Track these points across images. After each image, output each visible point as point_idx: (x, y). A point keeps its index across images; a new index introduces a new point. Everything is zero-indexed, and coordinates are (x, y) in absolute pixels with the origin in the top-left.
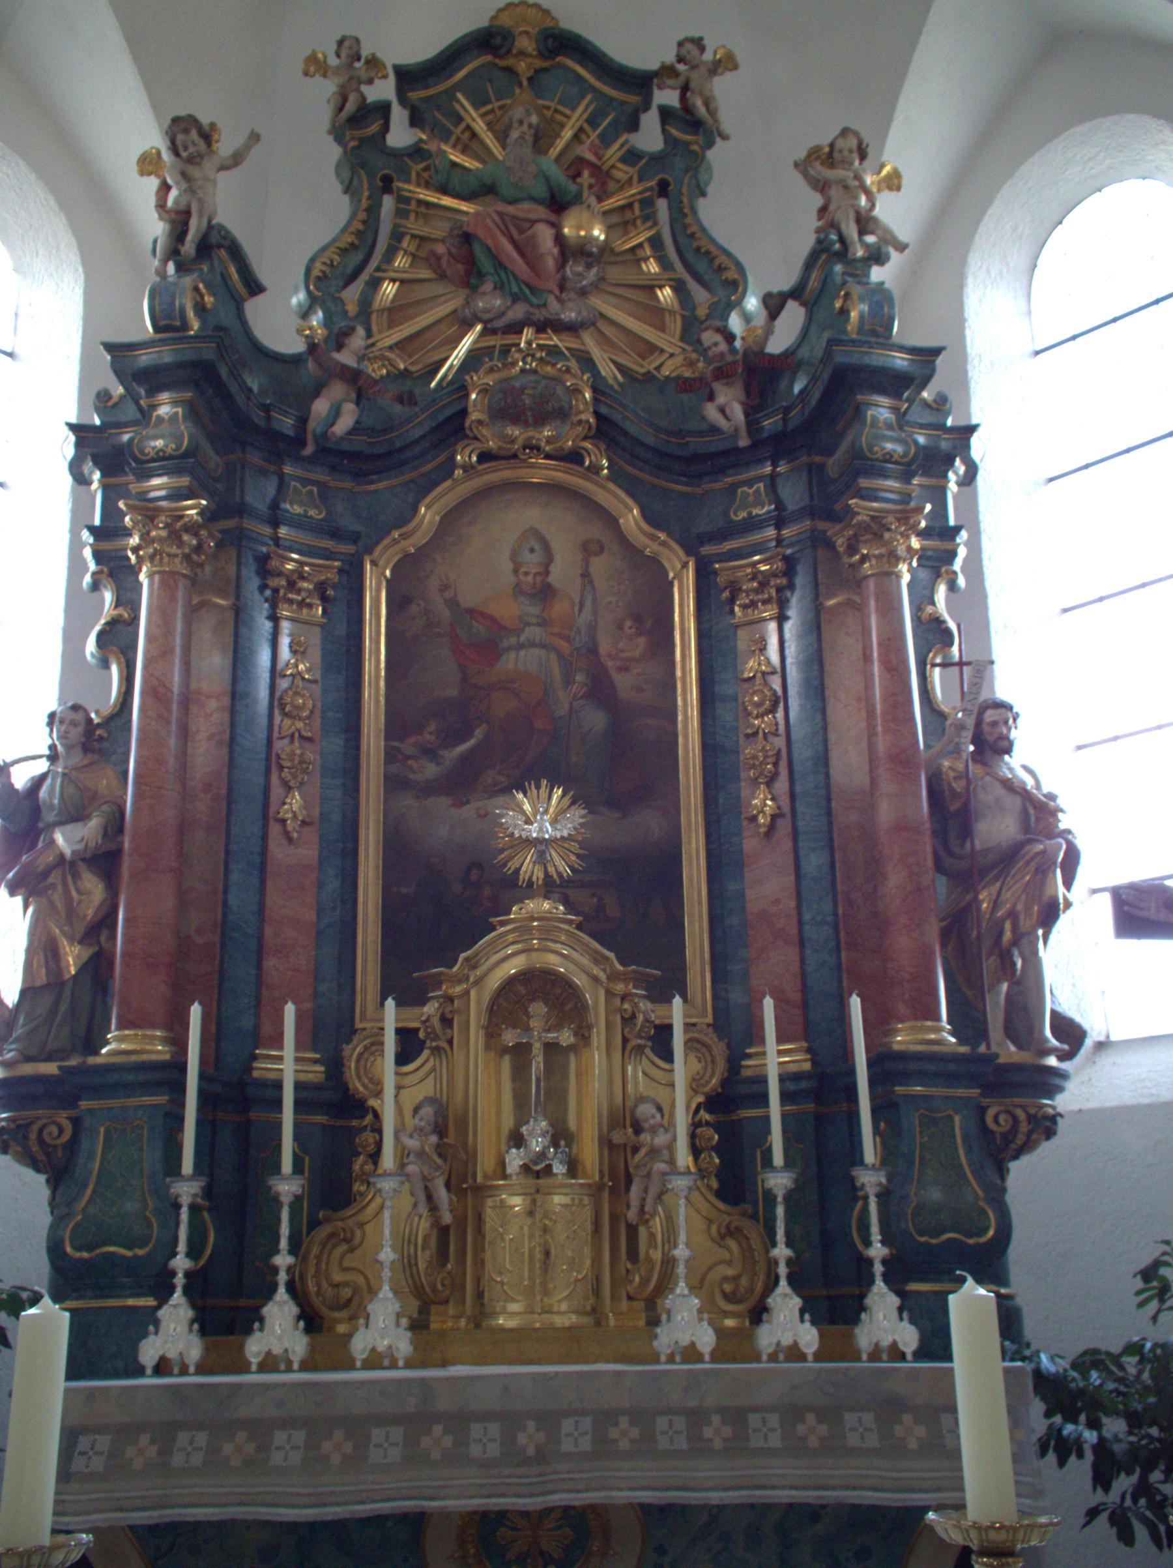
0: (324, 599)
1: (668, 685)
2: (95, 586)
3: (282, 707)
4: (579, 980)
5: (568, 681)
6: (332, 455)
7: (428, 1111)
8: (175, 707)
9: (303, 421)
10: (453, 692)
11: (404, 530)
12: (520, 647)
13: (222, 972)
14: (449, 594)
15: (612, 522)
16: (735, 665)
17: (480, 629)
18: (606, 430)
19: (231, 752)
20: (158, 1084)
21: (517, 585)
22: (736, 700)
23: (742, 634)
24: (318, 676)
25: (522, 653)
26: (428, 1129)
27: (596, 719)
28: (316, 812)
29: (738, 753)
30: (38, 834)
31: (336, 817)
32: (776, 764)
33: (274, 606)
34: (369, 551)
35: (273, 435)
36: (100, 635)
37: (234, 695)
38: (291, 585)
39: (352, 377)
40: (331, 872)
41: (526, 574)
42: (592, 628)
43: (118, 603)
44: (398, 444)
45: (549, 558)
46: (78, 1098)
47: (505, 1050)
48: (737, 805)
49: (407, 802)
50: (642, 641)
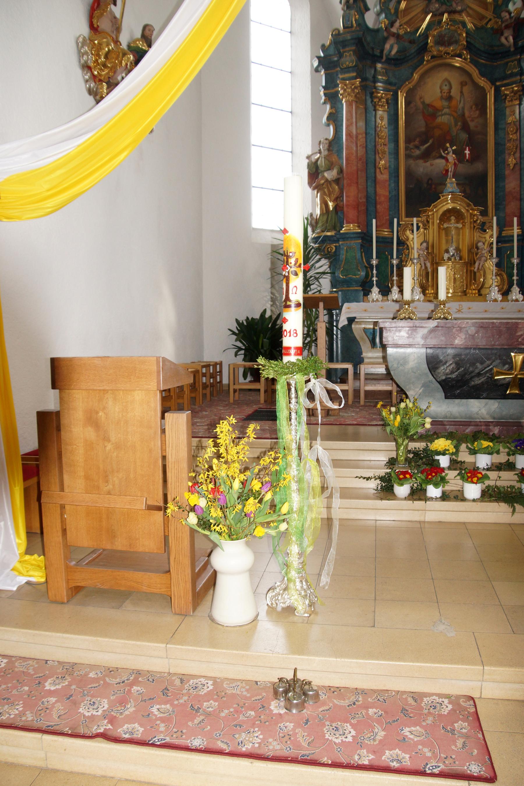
0: (387, 103)
1: (485, 125)
2: (325, 103)
3: (378, 136)
4: (463, 210)
5: (456, 125)
6: (390, 61)
7: (425, 244)
8: (354, 139)
9: (382, 51)
10: (423, 129)
11: (410, 81)
12: (442, 115)
13: (367, 209)
14: (422, 100)
15: (469, 75)
16: (505, 119)
17: (430, 110)
18: (469, 47)
19: (366, 150)
20: (359, 237)
21: (442, 96)
22: (505, 129)
23: (508, 109)
24: (387, 126)
25: (443, 117)
26: (425, 248)
27: (464, 136)
28: (388, 165)
29: (505, 145)
30: (318, 174)
31: (393, 166)
32: (516, 149)
33: (375, 106)
34: (399, 88)
35: (374, 56)
36: (327, 118)
37: (366, 134)
38: (380, 100)
39: (398, 36)
40: (392, 181)
41: (444, 93)
42: (463, 108)
43: (331, 108)
44: (408, 55)
45: (451, 88)
46: (339, 241)
47: (444, 229)
48: (504, 161)
49: (411, 161)
50: (478, 112)
